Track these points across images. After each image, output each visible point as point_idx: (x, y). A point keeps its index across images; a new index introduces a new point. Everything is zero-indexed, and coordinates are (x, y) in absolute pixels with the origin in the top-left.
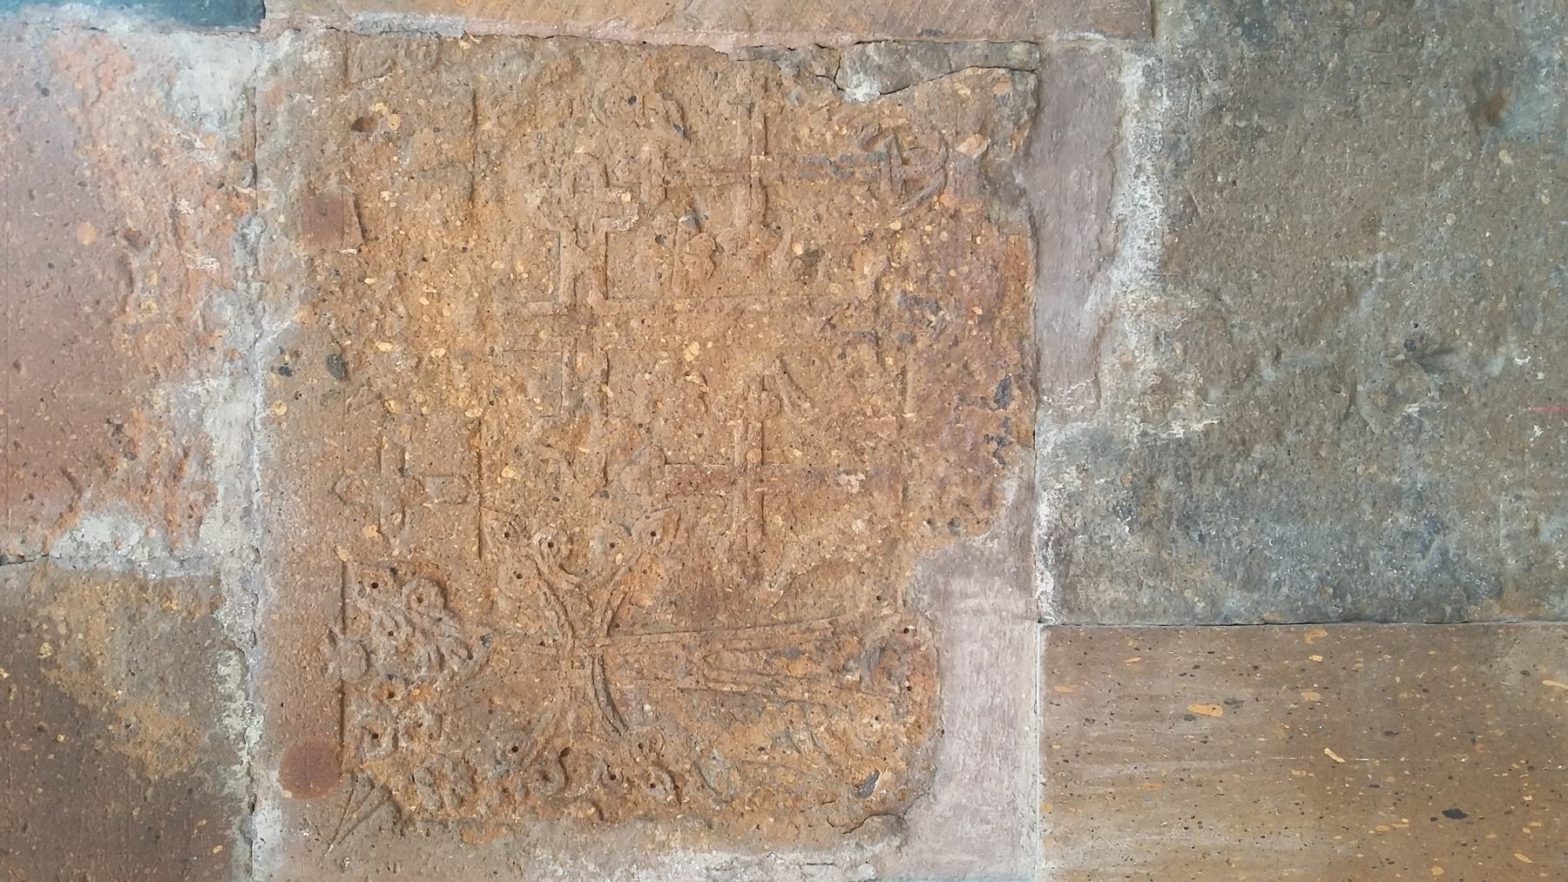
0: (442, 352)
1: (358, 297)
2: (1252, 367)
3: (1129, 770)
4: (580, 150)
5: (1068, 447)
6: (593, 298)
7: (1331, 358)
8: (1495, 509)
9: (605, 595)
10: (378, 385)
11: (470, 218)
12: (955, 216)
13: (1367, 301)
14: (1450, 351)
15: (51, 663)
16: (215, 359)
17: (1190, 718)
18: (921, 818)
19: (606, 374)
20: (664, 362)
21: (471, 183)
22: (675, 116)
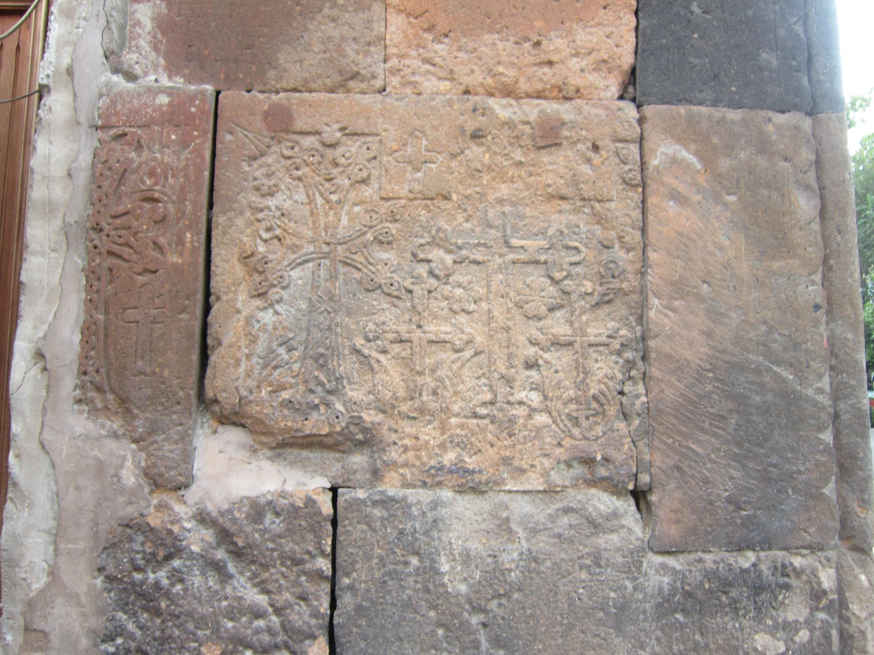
0: (485, 182)
1: (511, 144)
9: (362, 259)
22: (606, 298)
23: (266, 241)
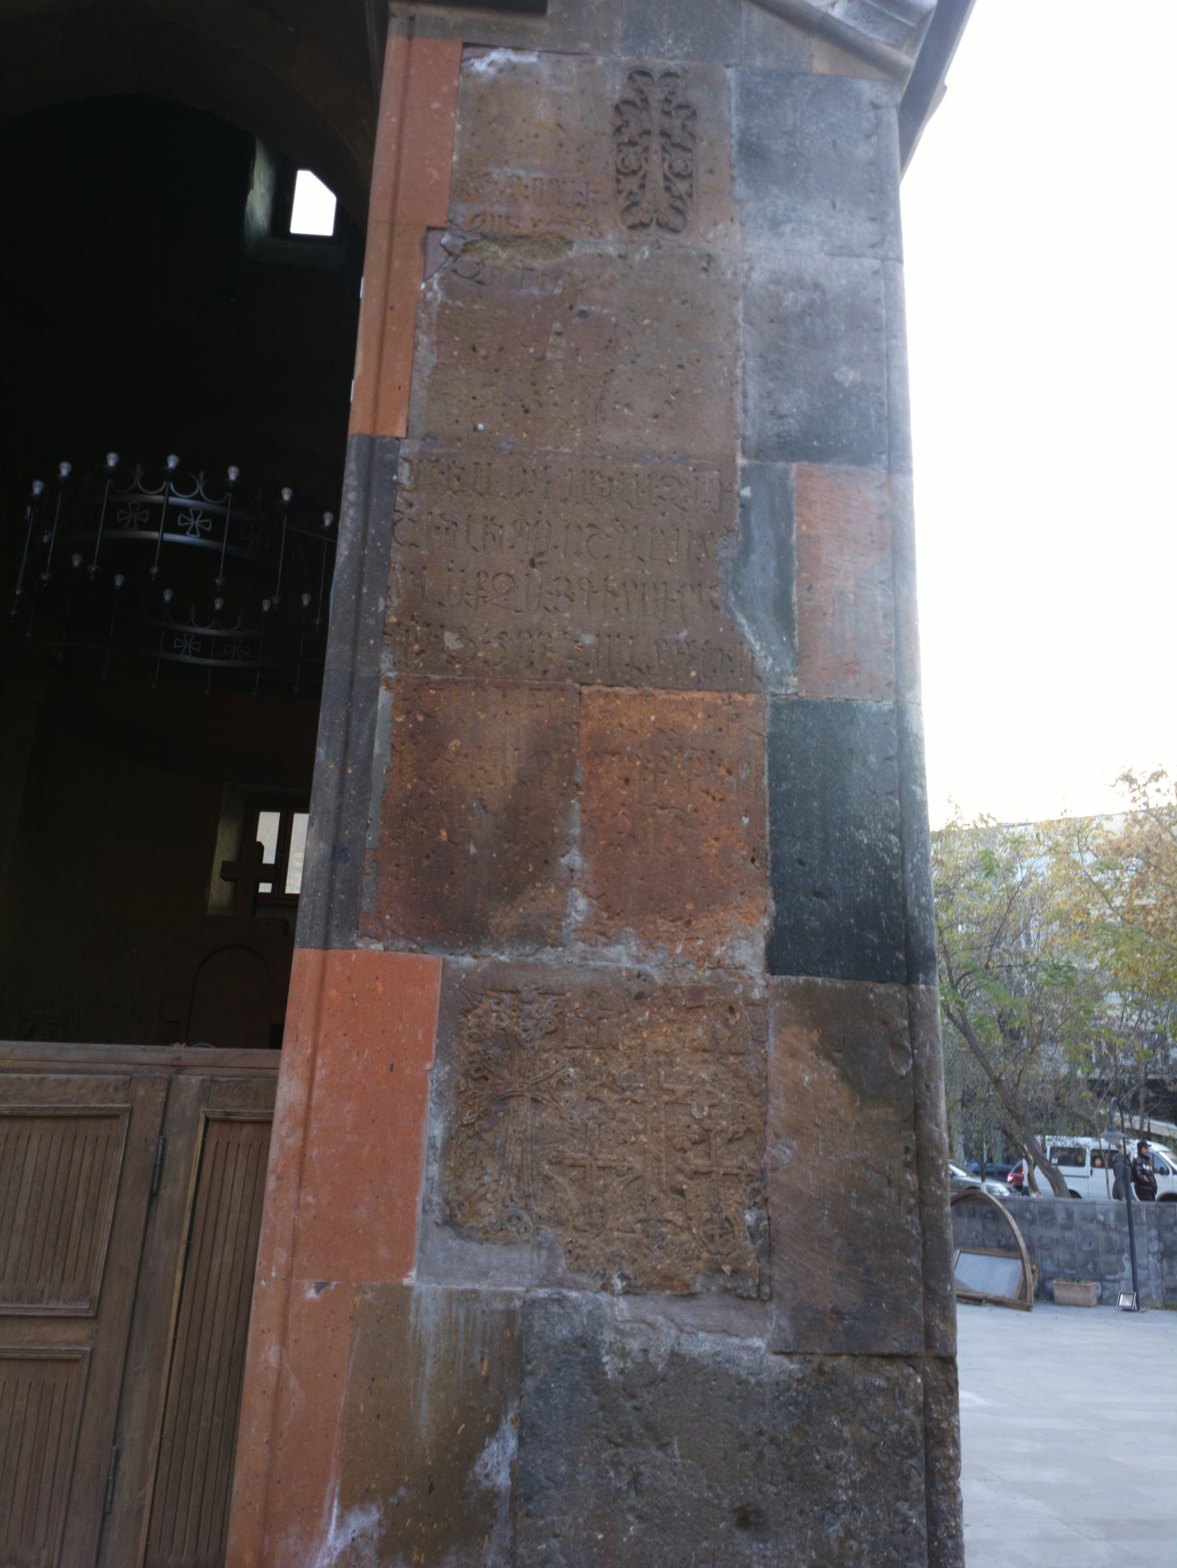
1: (666, 1005)
2: (633, 1396)
3: (461, 1329)
4: (723, 1095)
5: (599, 1307)
6: (666, 1098)
7: (635, 1435)
8: (566, 1514)
9: (548, 1097)
10: (633, 1011)
11: (696, 1050)
12: (699, 1258)
13: (660, 1454)
14: (637, 1494)
15: (534, 886)
16: (643, 950)
17: (482, 1360)
18: (449, 1232)
19: (635, 1102)
20: (640, 1126)
21: (712, 1049)
22: (738, 1136)
23: (475, 1080)
